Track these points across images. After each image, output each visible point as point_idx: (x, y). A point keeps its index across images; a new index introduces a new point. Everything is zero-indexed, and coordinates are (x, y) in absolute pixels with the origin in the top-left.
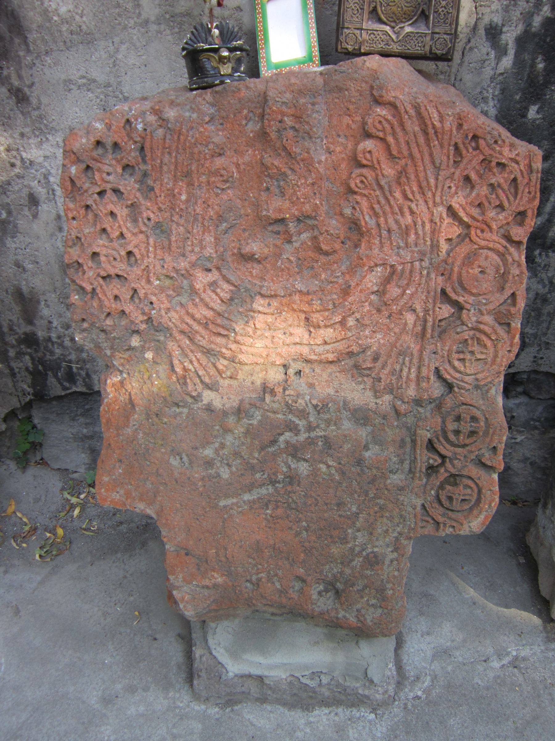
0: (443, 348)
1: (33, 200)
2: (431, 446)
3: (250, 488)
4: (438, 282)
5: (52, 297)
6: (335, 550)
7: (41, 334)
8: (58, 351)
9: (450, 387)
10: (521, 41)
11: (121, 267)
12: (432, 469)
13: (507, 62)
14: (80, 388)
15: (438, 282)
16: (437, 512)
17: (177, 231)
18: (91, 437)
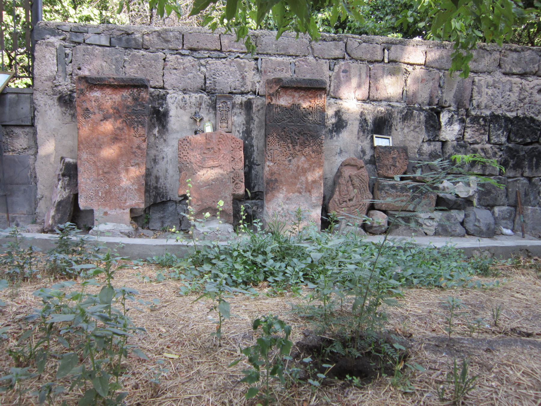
0: (233, 164)
1: (163, 158)
2: (233, 178)
3: (205, 186)
4: (231, 155)
5: (163, 177)
6: (220, 196)
7: (159, 186)
8: (161, 190)
9: (234, 169)
10: (243, 132)
11: (186, 154)
12: (233, 182)
13: (241, 135)
14: (164, 200)
15: (231, 155)
16: (235, 189)
17: (194, 150)
18: (163, 217)
